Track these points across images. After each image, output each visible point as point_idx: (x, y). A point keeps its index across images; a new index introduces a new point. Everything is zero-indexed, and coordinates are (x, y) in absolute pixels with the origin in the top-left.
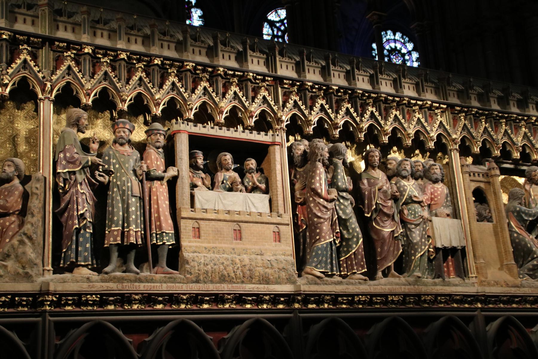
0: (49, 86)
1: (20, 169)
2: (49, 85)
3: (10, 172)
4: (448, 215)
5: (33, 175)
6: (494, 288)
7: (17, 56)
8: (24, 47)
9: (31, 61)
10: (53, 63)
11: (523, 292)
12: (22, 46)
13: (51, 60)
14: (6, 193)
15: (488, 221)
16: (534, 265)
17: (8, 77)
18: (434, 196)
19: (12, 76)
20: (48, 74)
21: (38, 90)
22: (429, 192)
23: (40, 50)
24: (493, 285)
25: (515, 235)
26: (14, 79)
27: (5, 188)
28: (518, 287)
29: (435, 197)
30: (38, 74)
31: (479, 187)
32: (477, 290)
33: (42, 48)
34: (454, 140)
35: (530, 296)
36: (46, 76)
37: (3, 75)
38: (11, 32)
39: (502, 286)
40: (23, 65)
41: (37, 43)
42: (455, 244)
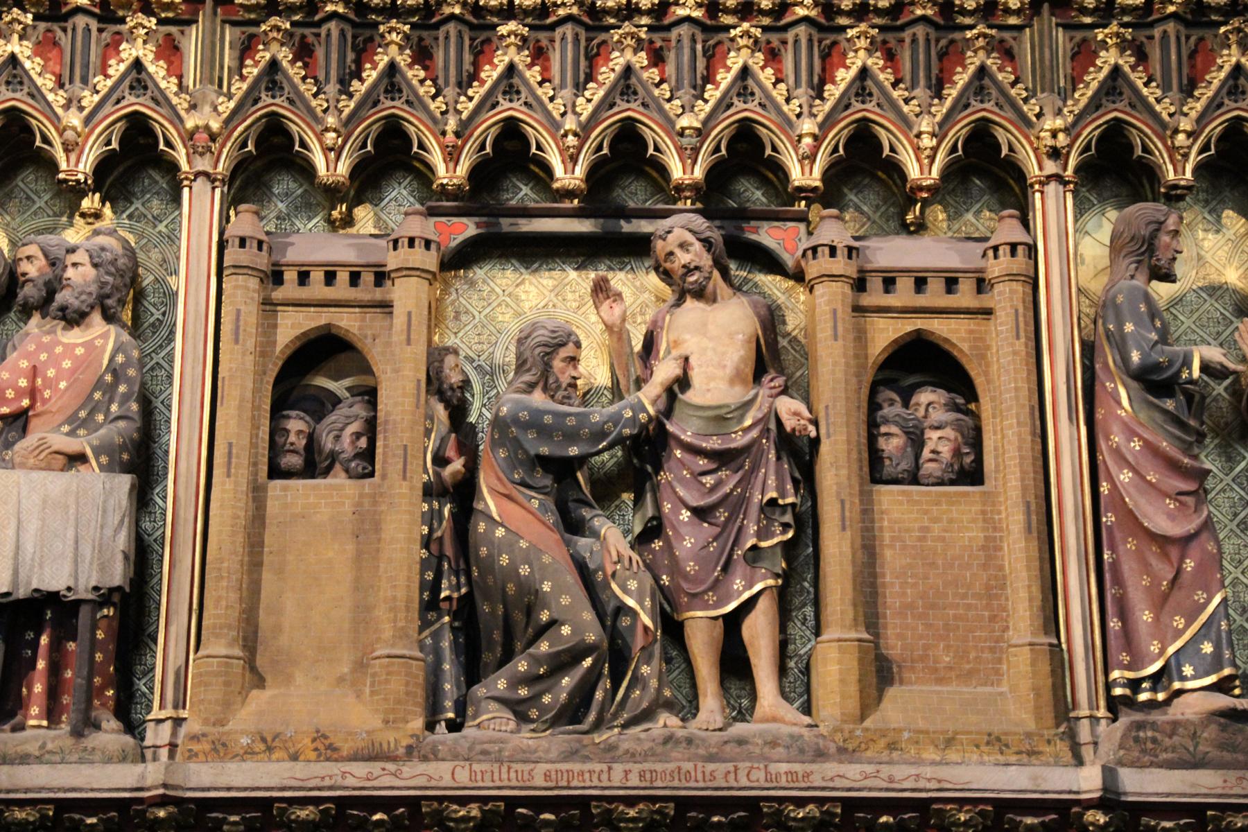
4: (77, 459)
6: (247, 766)
11: (422, 781)
15: (350, 474)
16: (536, 660)
18: (45, 378)
22: (24, 364)
24: (249, 753)
25: (482, 527)
28: (393, 759)
29: (49, 384)
31: (328, 326)
32: (143, 777)
34: (191, 135)
35: (463, 801)
39: (295, 758)
42: (55, 579)
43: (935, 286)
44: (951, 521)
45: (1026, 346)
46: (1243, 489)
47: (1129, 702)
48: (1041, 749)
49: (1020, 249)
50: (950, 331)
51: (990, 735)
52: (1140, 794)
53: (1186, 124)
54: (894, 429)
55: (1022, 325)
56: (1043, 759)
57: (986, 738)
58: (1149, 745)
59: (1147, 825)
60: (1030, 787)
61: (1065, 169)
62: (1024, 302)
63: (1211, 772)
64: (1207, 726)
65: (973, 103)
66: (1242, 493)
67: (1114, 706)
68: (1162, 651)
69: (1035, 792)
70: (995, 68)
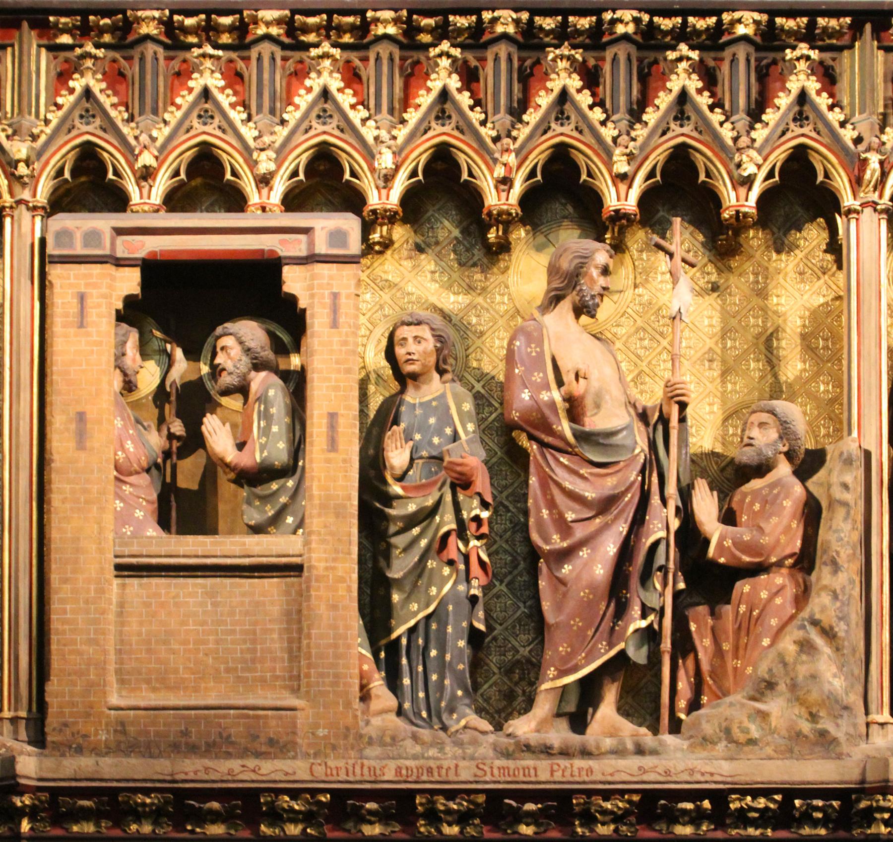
0: (877, 166)
1: (794, 433)
2: (874, 160)
3: (767, 445)
5: (829, 449)
7: (778, 85)
8: (797, 53)
9: (818, 93)
10: (886, 89)
12: (794, 48)
13: (880, 80)
14: (757, 507)
17: (753, 153)
19: (765, 150)
20: (872, 129)
21: (841, 183)
23: (846, 53)
26: (772, 158)
27: (756, 493)
30: (842, 131)
33: (851, 47)
36: (865, 135)
37: (738, 150)
38: (760, 11)
40: (797, 108)
41: (838, 34)
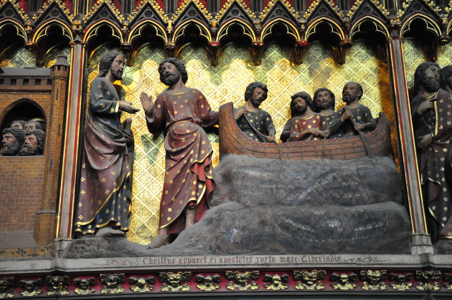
43: (32, 82)
44: (25, 169)
45: (60, 102)
46: (152, 157)
47: (80, 234)
48: (39, 253)
49: (62, 67)
50: (37, 99)
51: (19, 249)
52: (74, 269)
53: (126, 23)
54: (11, 135)
55: (59, 95)
56: (38, 257)
57: (17, 250)
58: (81, 250)
59: (76, 281)
60: (30, 269)
61: (83, 40)
62: (61, 86)
63: (103, 259)
64: (103, 241)
65: (51, 16)
66: (151, 159)
67: (76, 235)
68: (94, 213)
69: (32, 270)
70: (59, 3)
